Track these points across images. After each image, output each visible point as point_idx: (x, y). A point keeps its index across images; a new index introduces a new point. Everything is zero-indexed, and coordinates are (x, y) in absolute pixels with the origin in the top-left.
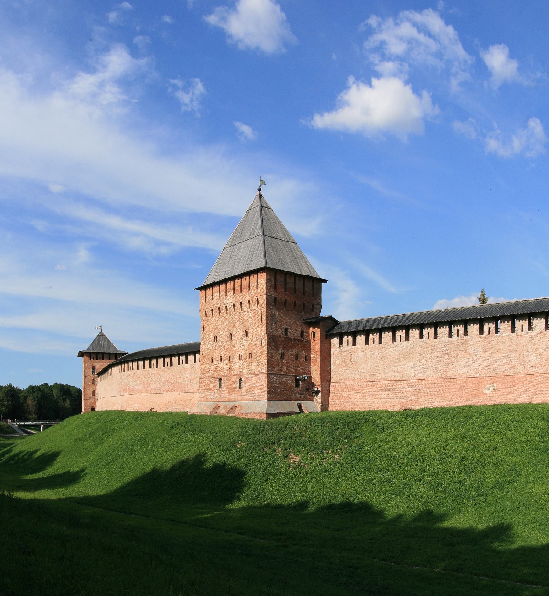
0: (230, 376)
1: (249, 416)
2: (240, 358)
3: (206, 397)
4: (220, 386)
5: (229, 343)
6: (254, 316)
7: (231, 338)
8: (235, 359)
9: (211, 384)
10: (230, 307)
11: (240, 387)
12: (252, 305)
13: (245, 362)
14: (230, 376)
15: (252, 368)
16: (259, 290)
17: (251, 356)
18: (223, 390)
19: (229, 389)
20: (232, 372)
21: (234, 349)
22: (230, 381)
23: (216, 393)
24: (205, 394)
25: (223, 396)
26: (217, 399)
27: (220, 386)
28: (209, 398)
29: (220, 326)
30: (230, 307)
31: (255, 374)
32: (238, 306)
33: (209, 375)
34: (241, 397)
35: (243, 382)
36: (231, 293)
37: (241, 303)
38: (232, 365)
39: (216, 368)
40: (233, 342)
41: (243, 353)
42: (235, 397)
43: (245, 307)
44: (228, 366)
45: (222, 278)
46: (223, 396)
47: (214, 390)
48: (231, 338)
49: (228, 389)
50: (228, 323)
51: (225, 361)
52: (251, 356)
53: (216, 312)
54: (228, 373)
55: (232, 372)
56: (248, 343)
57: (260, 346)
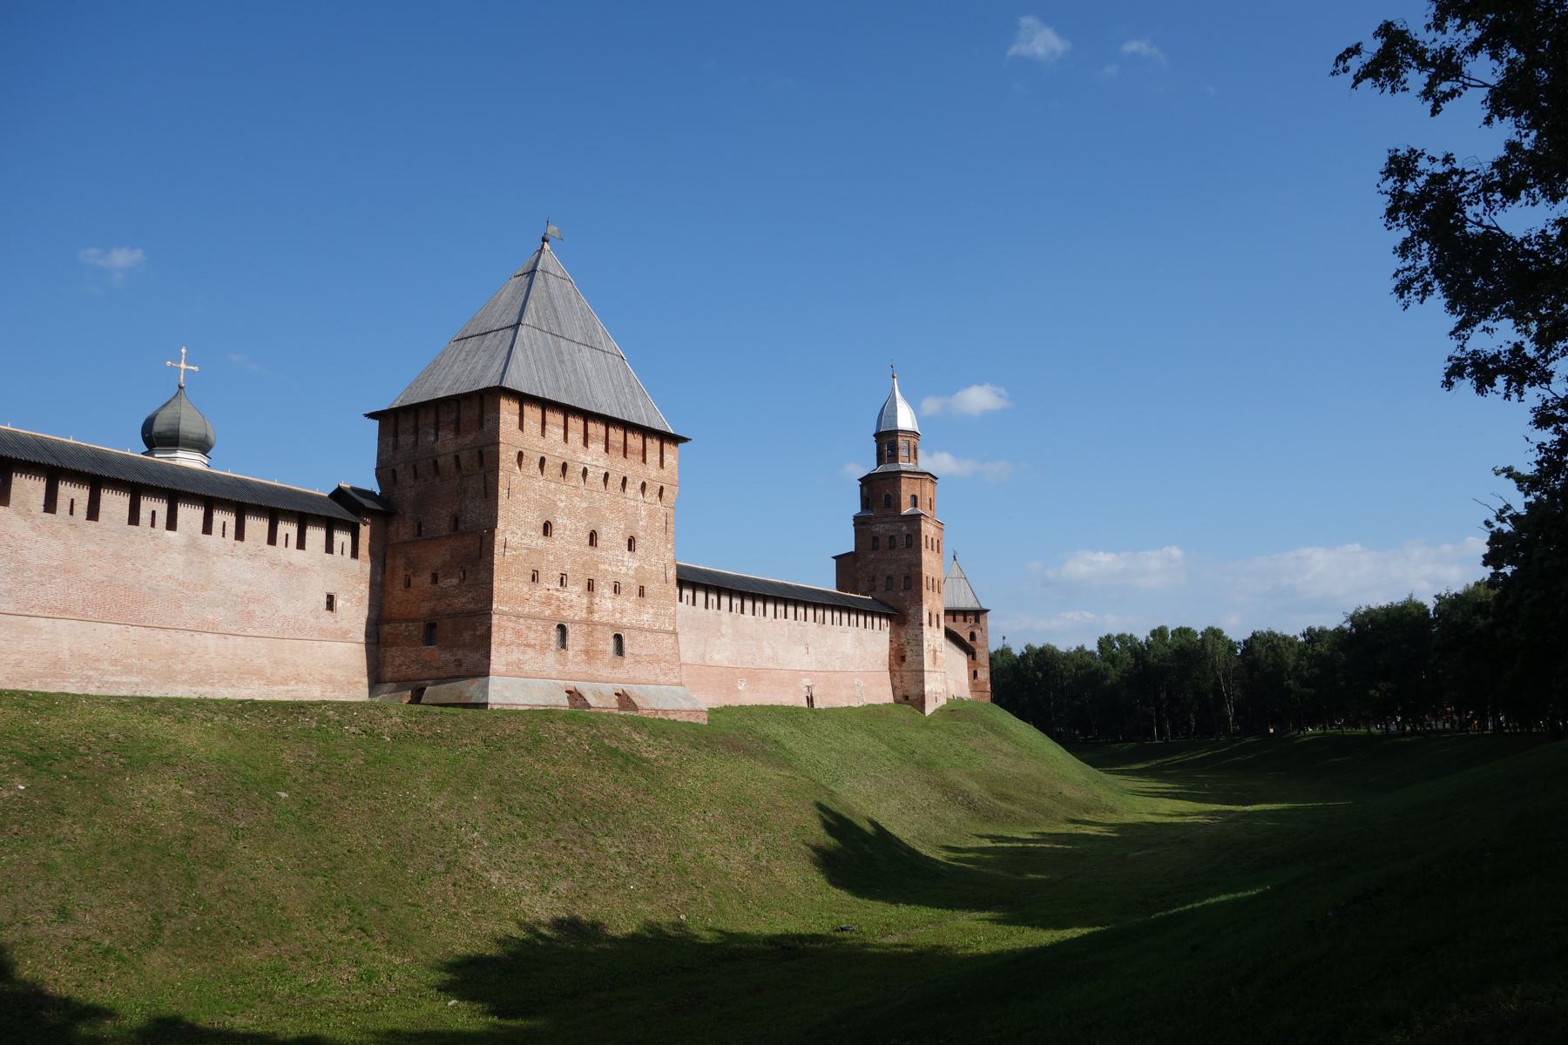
0: (588, 623)
1: (672, 717)
2: (617, 589)
3: (519, 663)
5: (588, 549)
6: (651, 515)
9: (532, 635)
10: (595, 475)
11: (620, 650)
12: (647, 493)
13: (629, 602)
14: (588, 623)
15: (645, 617)
16: (665, 473)
17: (642, 592)
18: (570, 653)
19: (590, 654)
20: (596, 617)
21: (601, 567)
22: (590, 634)
23: (551, 658)
24: (514, 657)
25: (571, 667)
26: (554, 674)
28: (527, 667)
29: (562, 505)
30: (595, 475)
31: (652, 631)
32: (615, 481)
34: (620, 674)
35: (626, 642)
36: (597, 447)
37: (625, 479)
38: (597, 600)
39: (549, 598)
40: (597, 552)
41: (622, 581)
42: (605, 672)
43: (633, 489)
44: (585, 600)
46: (571, 667)
47: (543, 649)
49: (587, 652)
50: (584, 505)
52: (642, 592)
54: (584, 615)
55: (596, 617)
56: (636, 565)
57: (662, 577)
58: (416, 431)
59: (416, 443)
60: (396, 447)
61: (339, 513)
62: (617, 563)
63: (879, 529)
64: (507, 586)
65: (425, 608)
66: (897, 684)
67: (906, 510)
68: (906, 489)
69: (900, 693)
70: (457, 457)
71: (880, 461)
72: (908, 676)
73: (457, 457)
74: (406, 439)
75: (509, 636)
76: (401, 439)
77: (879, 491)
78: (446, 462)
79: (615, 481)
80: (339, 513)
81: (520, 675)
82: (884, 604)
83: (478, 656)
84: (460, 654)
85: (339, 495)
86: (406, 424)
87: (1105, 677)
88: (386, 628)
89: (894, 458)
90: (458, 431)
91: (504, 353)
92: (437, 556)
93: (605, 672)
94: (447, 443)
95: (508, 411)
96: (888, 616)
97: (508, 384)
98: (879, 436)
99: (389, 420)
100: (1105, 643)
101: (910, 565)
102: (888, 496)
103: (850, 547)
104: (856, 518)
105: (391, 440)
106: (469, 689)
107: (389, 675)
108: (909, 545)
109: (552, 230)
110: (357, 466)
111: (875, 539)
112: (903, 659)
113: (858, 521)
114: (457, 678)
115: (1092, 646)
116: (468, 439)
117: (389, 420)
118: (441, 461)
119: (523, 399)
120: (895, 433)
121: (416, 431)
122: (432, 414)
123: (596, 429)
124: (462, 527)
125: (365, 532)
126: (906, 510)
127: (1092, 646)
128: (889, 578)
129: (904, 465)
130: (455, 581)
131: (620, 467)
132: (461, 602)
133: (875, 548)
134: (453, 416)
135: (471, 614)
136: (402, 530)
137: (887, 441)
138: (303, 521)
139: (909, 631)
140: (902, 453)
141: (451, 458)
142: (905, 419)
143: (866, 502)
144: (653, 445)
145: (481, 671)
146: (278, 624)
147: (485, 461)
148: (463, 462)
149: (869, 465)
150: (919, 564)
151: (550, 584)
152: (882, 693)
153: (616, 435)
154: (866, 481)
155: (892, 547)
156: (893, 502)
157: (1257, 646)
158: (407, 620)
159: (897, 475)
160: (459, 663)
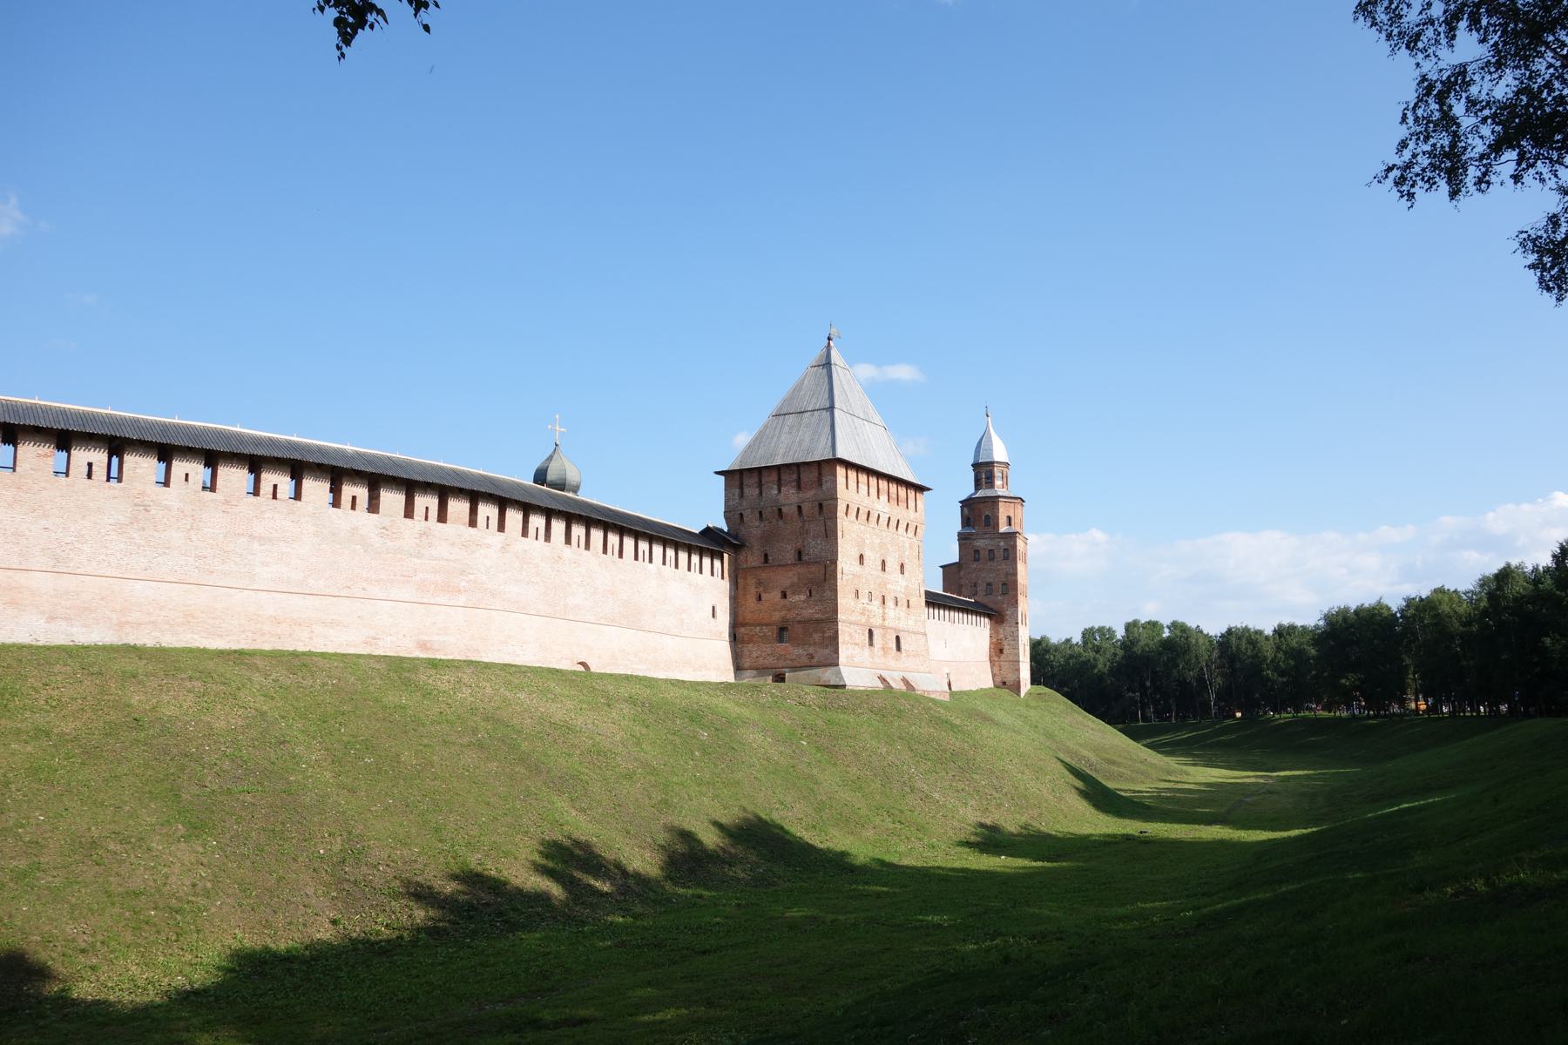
0: (883, 627)
3: (852, 656)
4: (871, 644)
5: (881, 573)
7: (883, 569)
8: (890, 603)
11: (899, 648)
15: (911, 622)
23: (867, 650)
27: (871, 644)
32: (893, 523)
33: (853, 618)
36: (884, 497)
42: (892, 663)
45: (858, 462)
48: (883, 569)
51: (877, 602)
53: (863, 516)
58: (760, 485)
60: (742, 495)
61: (708, 543)
62: (897, 584)
63: (980, 543)
64: (845, 601)
65: (777, 616)
66: (996, 670)
67: (1003, 528)
68: (1003, 511)
69: (999, 679)
71: (978, 485)
72: (1005, 666)
74: (751, 492)
75: (847, 638)
76: (746, 491)
77: (979, 515)
78: (789, 510)
79: (893, 523)
80: (708, 543)
81: (858, 666)
82: (984, 606)
84: (811, 650)
85: (708, 532)
86: (751, 481)
87: (1095, 666)
88: (742, 630)
89: (990, 484)
90: (799, 487)
91: (828, 429)
92: (786, 578)
93: (892, 663)
94: (789, 496)
95: (840, 471)
96: (989, 616)
97: (840, 455)
98: (976, 466)
99: (735, 478)
100: (1088, 634)
101: (1007, 574)
102: (987, 517)
103: (953, 556)
104: (959, 534)
105: (737, 491)
106: (827, 675)
107: (747, 665)
108: (1006, 558)
109: (833, 331)
110: (705, 509)
111: (977, 552)
112: (1001, 651)
113: (962, 538)
114: (811, 667)
115: (1077, 639)
116: (810, 494)
117: (735, 478)
118: (784, 509)
119: (849, 465)
120: (991, 464)
121: (760, 485)
122: (774, 476)
123: (883, 484)
124: (805, 558)
125: (726, 556)
126: (1003, 528)
127: (1077, 639)
128: (989, 584)
129: (1001, 492)
130: (803, 597)
131: (898, 512)
132: (809, 612)
133: (977, 560)
134: (795, 476)
135: (818, 621)
136: (752, 558)
137: (984, 472)
138: (690, 549)
139: (1005, 630)
140: (998, 482)
142: (999, 453)
143: (966, 521)
144: (911, 493)
145: (833, 662)
146: (677, 623)
147: (826, 510)
148: (804, 511)
149: (967, 489)
150: (1015, 574)
151: (864, 599)
152: (987, 682)
153: (893, 487)
154: (967, 504)
155: (992, 559)
156: (992, 522)
157: (1233, 640)
158: (761, 625)
159: (995, 500)
160: (811, 657)
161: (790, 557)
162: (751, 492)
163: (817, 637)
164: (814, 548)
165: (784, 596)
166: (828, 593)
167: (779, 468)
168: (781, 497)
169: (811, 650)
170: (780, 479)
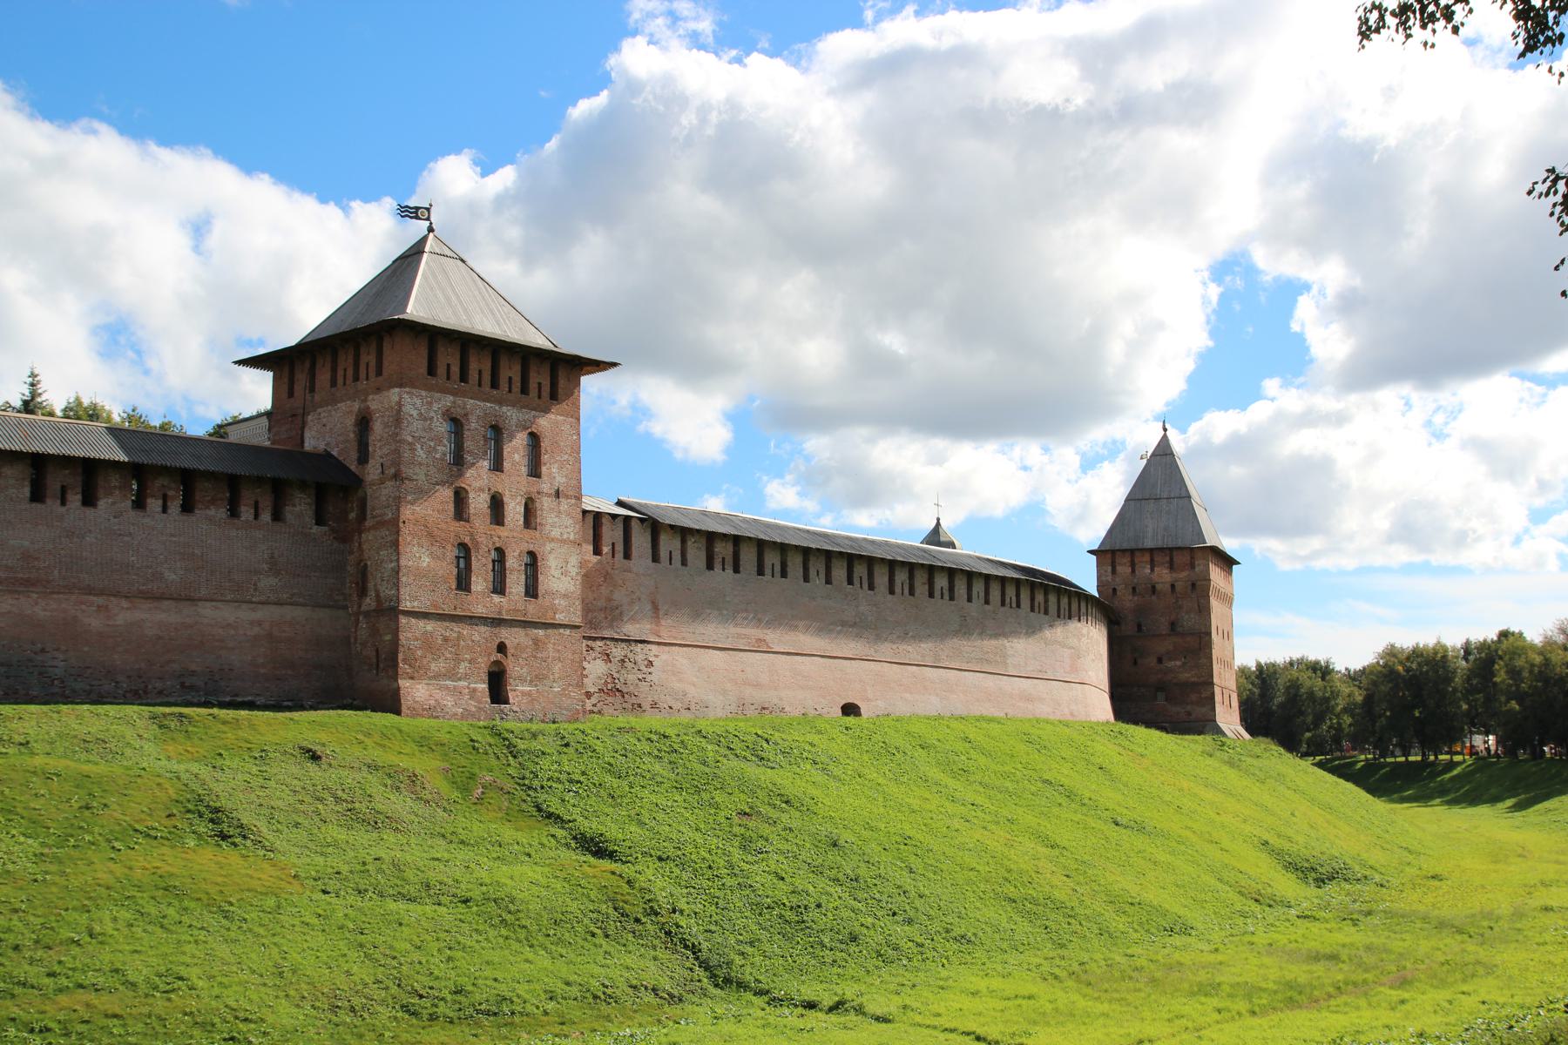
58: (1133, 565)
59: (1133, 571)
60: (1114, 572)
70: (1173, 586)
73: (1173, 586)
74: (1124, 569)
76: (1119, 569)
83: (1204, 710)
84: (1189, 708)
94: (1163, 576)
116: (1184, 574)
118: (1159, 587)
122: (1147, 557)
132: (1185, 676)
135: (1194, 684)
141: (1168, 586)
161: (1164, 628)
162: (1124, 569)
163: (1194, 697)
164: (1188, 620)
165: (1160, 660)
166: (1203, 661)
167: (1151, 551)
168: (1155, 577)
169: (1189, 708)
170: (1152, 561)
